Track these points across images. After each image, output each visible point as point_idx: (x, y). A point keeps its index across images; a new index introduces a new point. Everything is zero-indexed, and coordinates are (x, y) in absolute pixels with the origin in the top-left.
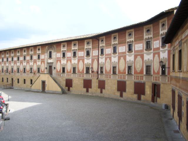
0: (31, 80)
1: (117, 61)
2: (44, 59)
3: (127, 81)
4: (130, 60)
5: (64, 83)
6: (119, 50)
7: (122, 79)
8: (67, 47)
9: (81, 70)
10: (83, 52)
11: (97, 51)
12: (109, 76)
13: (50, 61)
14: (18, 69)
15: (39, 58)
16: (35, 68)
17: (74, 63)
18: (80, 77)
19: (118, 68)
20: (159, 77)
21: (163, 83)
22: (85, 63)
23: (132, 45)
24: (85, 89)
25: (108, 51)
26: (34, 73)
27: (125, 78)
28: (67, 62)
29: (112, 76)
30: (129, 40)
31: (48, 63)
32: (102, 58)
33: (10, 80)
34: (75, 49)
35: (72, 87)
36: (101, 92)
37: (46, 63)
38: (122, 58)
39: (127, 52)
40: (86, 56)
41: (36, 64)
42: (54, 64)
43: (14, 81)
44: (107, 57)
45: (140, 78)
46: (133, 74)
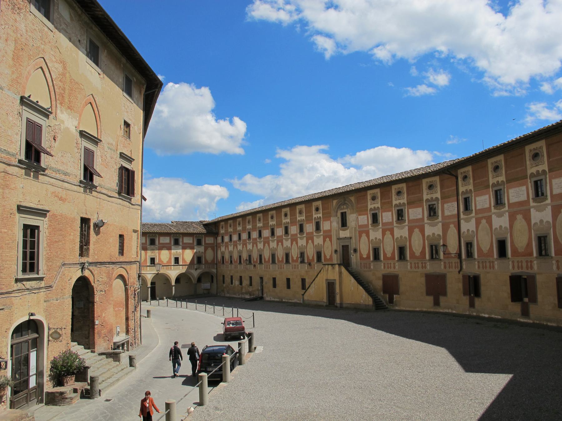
0: (303, 281)
2: (330, 231)
4: (541, 221)
5: (378, 284)
6: (510, 197)
7: (523, 271)
8: (381, 200)
9: (417, 250)
10: (420, 210)
11: (455, 204)
12: (488, 265)
13: (344, 234)
14: (273, 256)
15: (318, 228)
16: (311, 253)
17: (401, 237)
18: (417, 270)
19: (512, 242)
22: (427, 234)
23: (544, 181)
24: (430, 299)
26: (310, 264)
27: (532, 267)
28: (384, 234)
30: (534, 170)
31: (339, 239)
32: (467, 221)
33: (256, 280)
34: (400, 203)
35: (397, 293)
36: (472, 305)
37: (334, 239)
38: (519, 217)
39: (531, 201)
40: (428, 219)
41: (313, 242)
42: (353, 240)
43: (266, 283)
44: (480, 215)
46: (553, 254)
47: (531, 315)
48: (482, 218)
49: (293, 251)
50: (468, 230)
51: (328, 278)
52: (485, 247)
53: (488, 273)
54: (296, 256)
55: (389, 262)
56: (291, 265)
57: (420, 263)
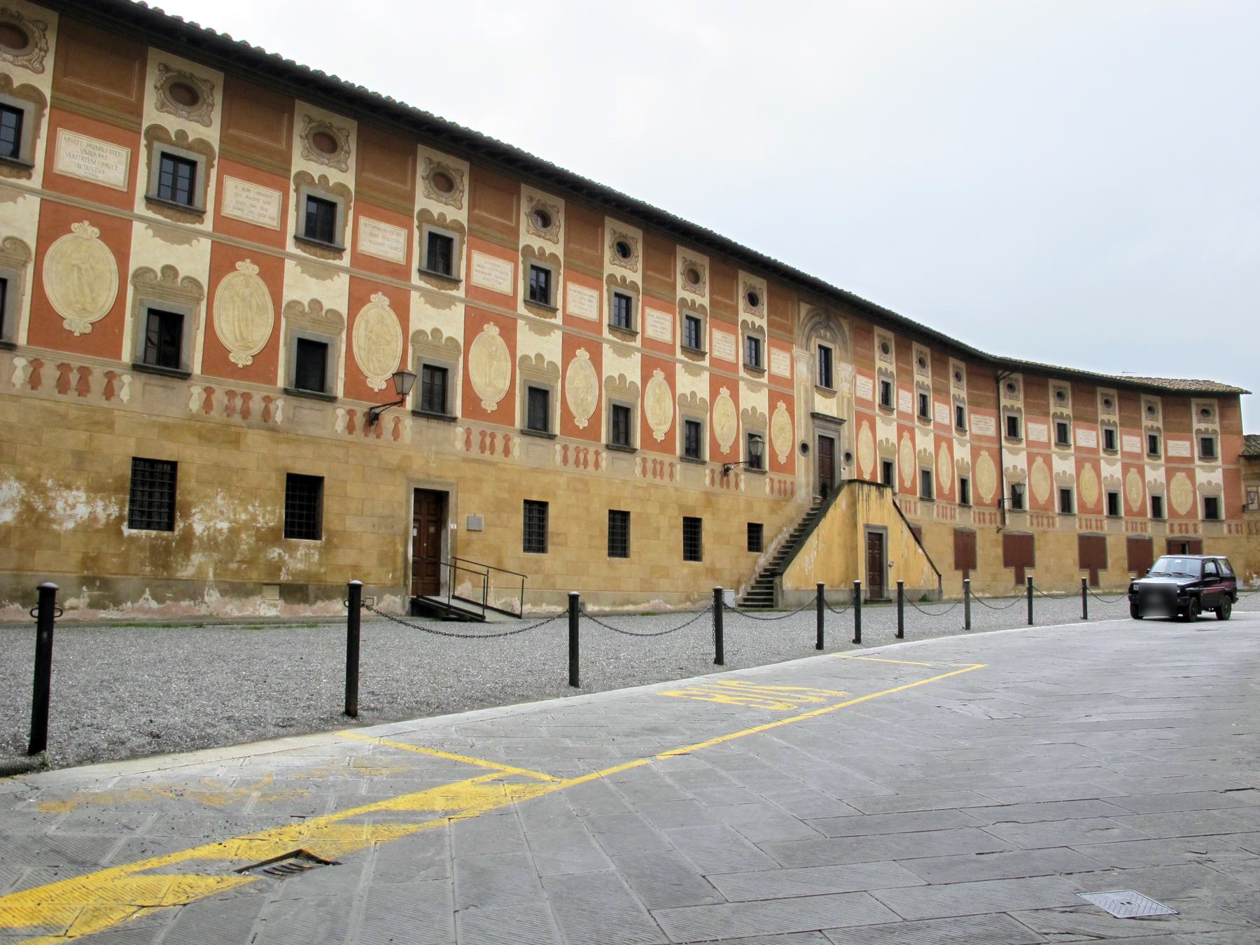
1: (1074, 472)
2: (790, 383)
3: (1110, 535)
6: (1078, 439)
7: (1094, 531)
11: (992, 422)
12: (1045, 521)
20: (1195, 525)
21: (1209, 538)
25: (1037, 431)
27: (1102, 528)
29: (1057, 519)
31: (815, 416)
38: (1088, 466)
42: (845, 429)
45: (1139, 526)
47: (1102, 583)
48: (1038, 454)
49: (649, 402)
50: (1015, 467)
51: (870, 523)
52: (1042, 497)
53: (1046, 532)
54: (666, 428)
55: (908, 500)
56: (638, 460)
57: (949, 509)
